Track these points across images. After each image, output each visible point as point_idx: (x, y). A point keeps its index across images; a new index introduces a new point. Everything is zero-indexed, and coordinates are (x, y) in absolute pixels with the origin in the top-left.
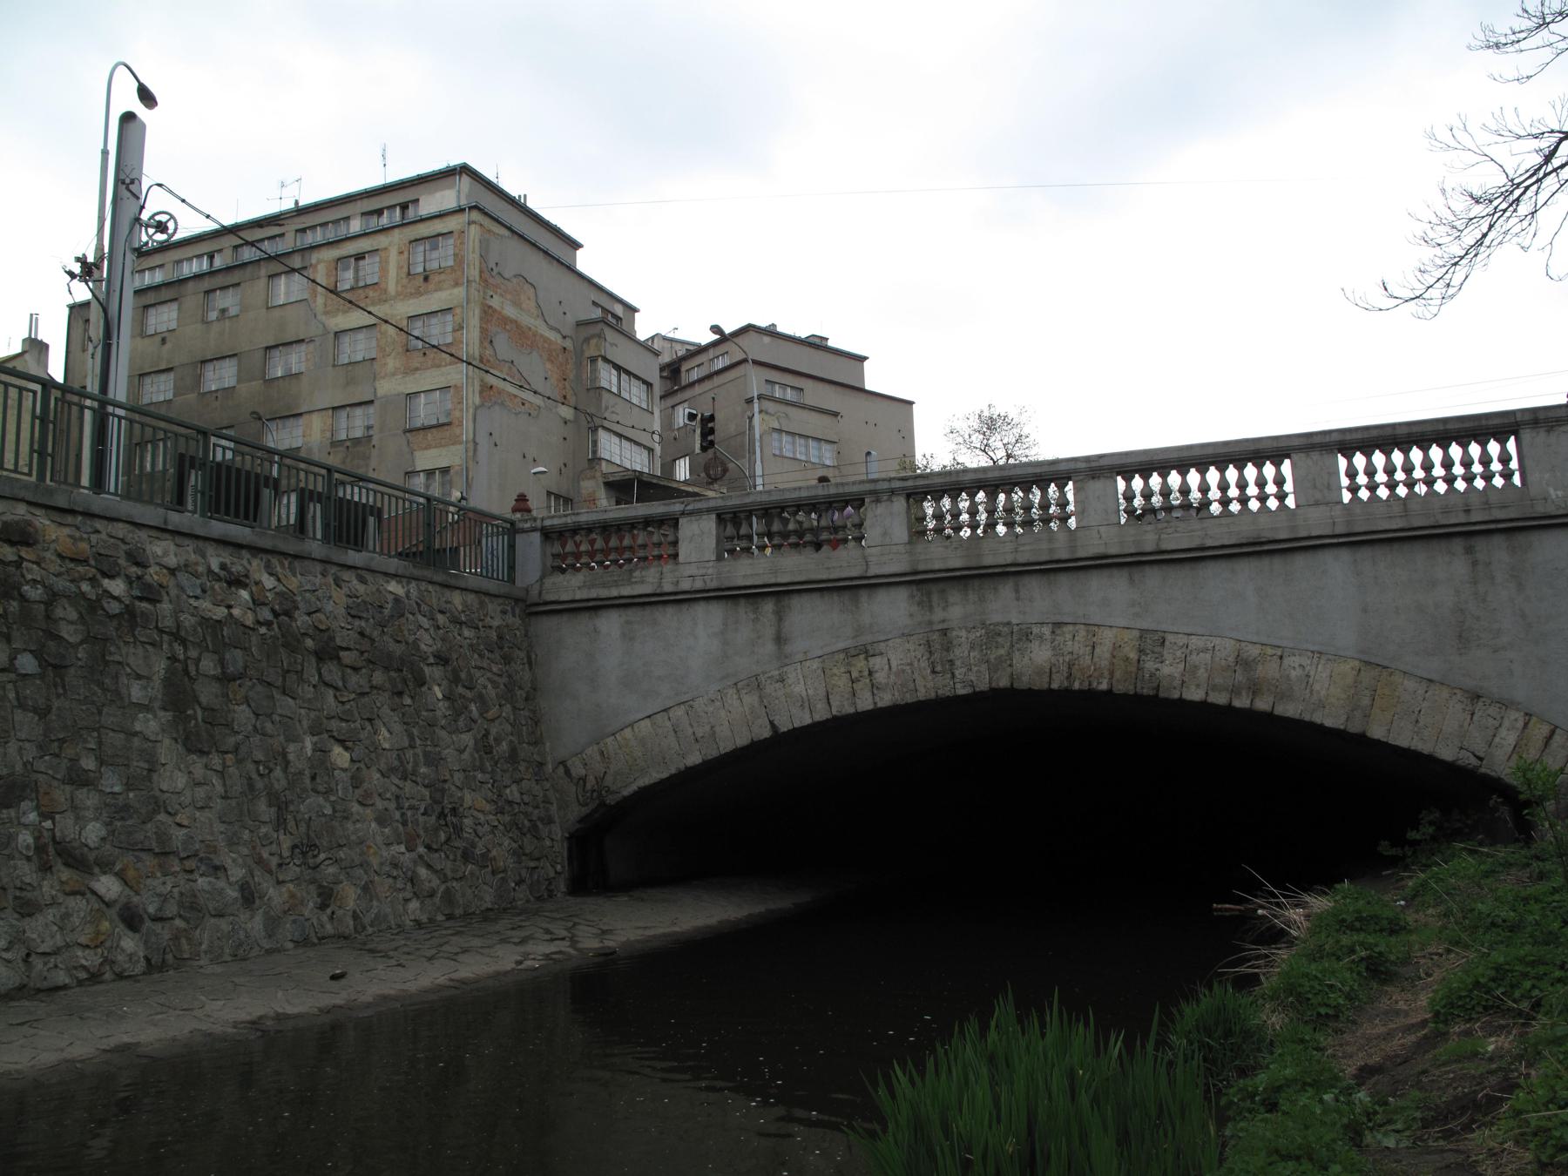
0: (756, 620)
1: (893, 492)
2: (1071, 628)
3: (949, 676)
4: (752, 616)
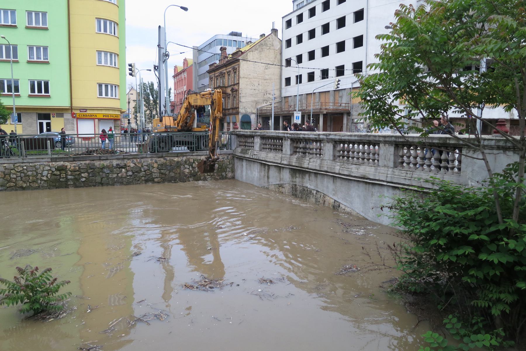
0: (265, 170)
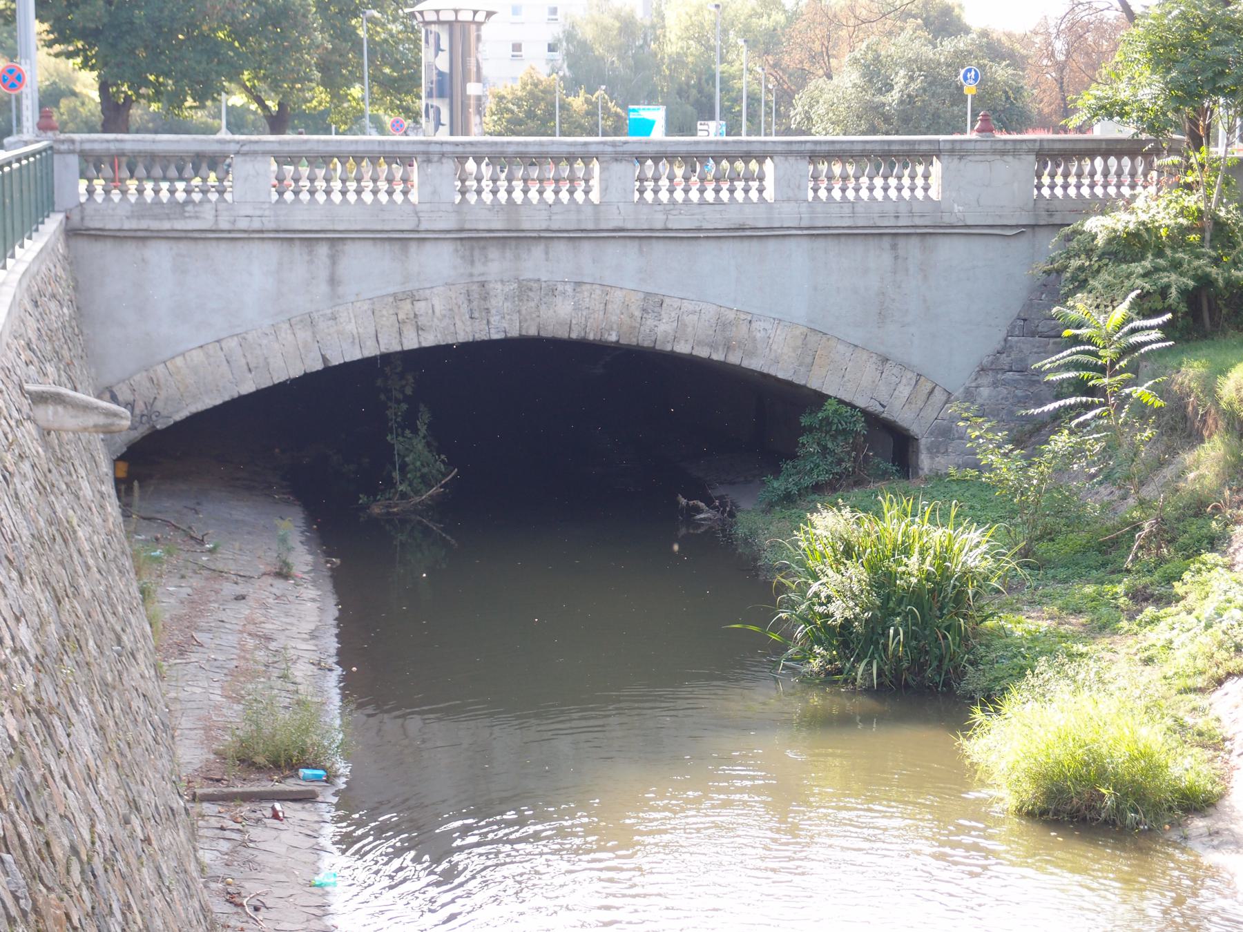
0: (311, 262)
1: (443, 155)
2: (588, 287)
3: (485, 322)
4: (306, 258)
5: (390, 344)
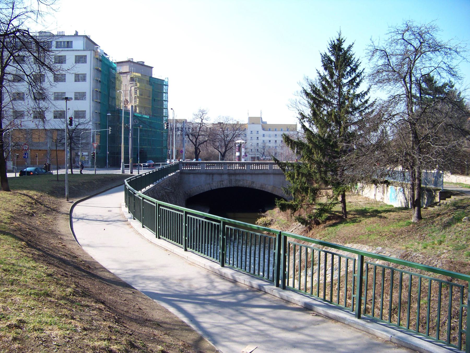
5: (219, 187)
